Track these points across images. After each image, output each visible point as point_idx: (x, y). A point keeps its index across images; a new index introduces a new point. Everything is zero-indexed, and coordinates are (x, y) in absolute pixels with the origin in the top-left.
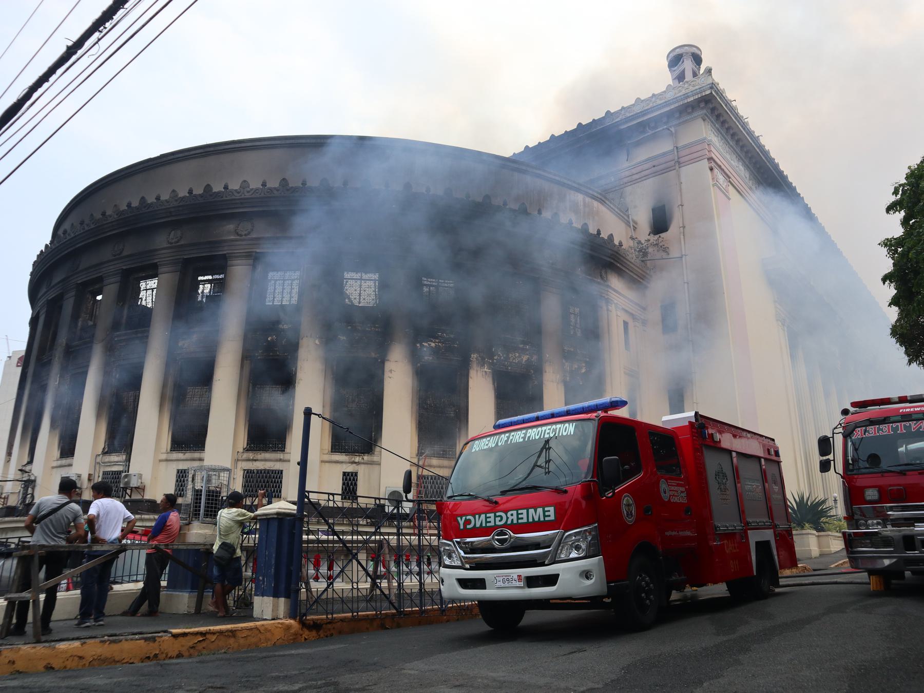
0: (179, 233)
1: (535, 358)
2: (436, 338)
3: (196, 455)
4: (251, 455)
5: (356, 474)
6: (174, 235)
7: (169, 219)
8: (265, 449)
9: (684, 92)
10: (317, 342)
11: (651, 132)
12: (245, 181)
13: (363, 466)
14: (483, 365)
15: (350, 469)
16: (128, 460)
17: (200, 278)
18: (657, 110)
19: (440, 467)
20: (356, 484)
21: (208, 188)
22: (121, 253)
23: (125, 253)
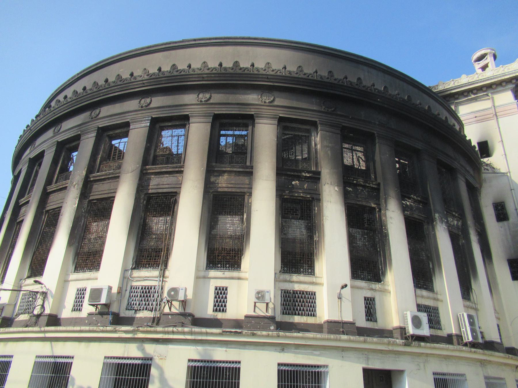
0: (208, 96)
1: (460, 223)
2: (410, 198)
3: (235, 274)
4: (287, 276)
5: (374, 299)
6: (204, 96)
7: (201, 83)
8: (297, 272)
9: (500, 72)
10: (336, 189)
11: (473, 96)
12: (268, 63)
13: (378, 293)
14: (442, 223)
15: (369, 294)
17: (222, 132)
18: (481, 82)
19: (428, 298)
21: (236, 63)
22: (149, 105)
23: (152, 106)
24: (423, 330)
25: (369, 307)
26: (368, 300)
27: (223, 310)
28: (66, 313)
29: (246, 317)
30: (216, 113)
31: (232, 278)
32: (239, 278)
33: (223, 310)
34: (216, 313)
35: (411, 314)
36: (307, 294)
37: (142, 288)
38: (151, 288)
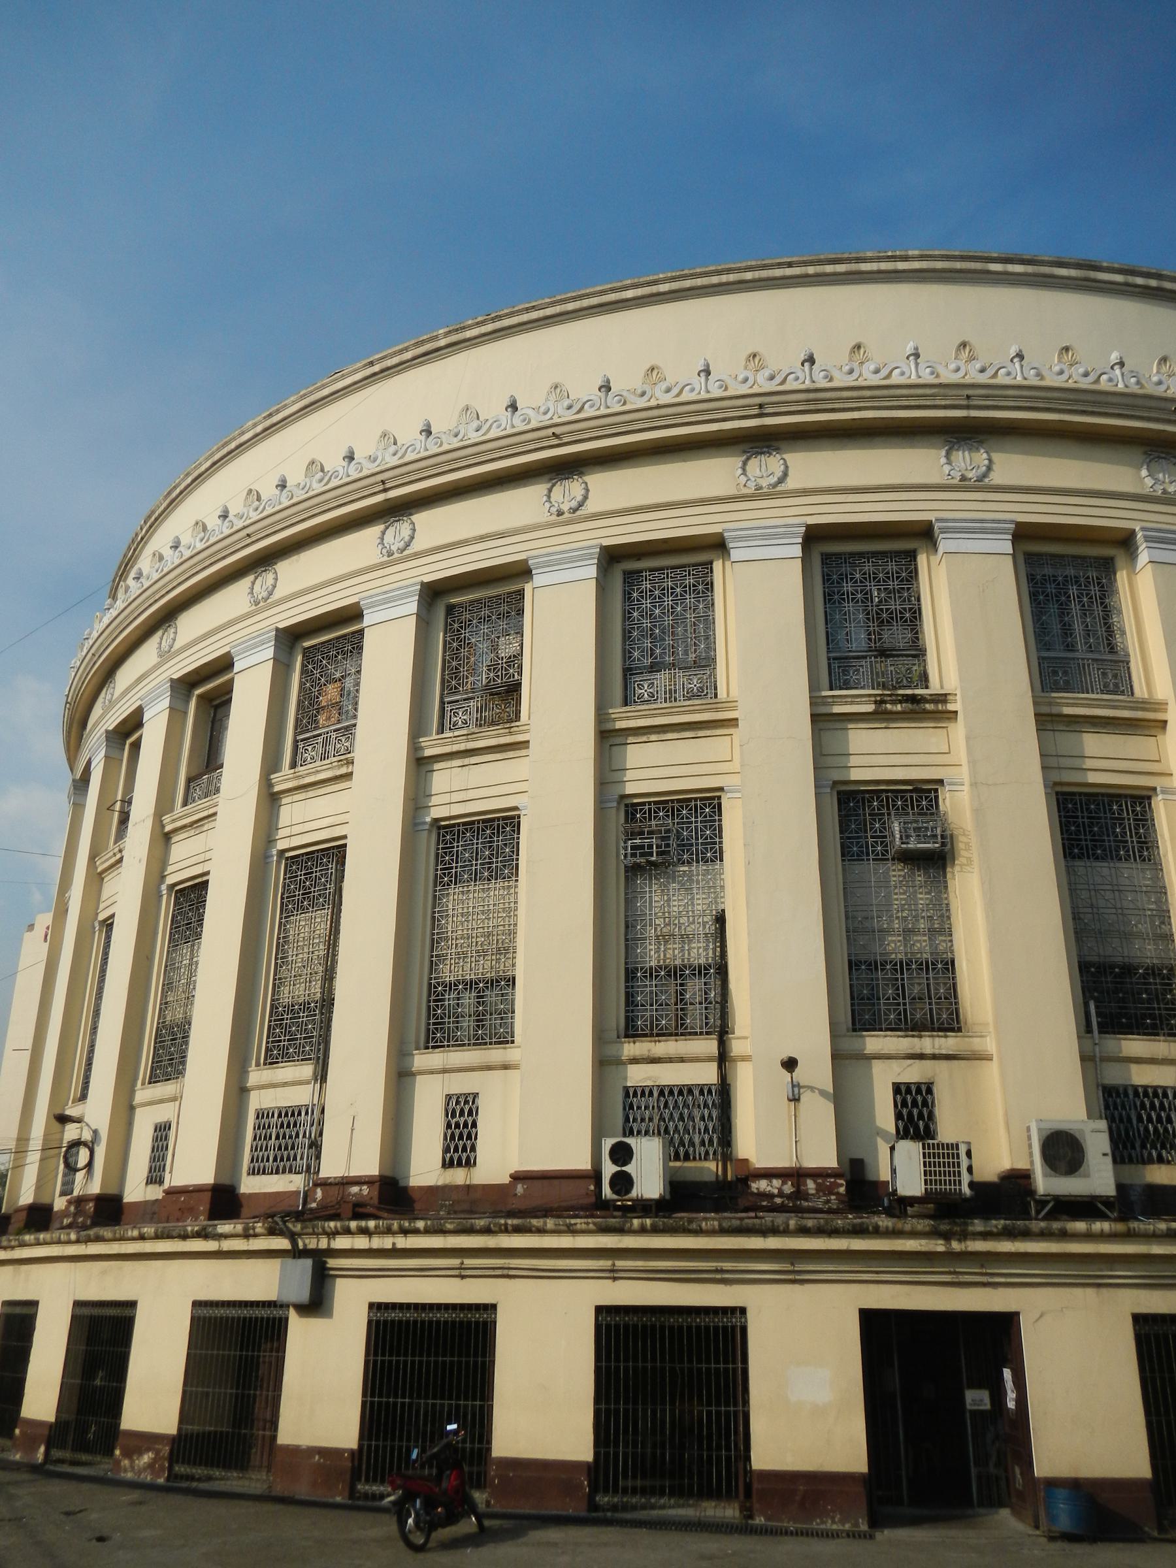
3: (495, 1054)
5: (929, 1091)
15: (912, 1073)
16: (321, 1076)
20: (931, 1116)
24: (1087, 1175)
25: (910, 1114)
26: (908, 1091)
27: (468, 1158)
28: (136, 1191)
29: (517, 1177)
30: (427, 579)
31: (489, 1068)
32: (506, 1067)
33: (468, 1158)
34: (450, 1171)
35: (1039, 1130)
36: (702, 1093)
37: (280, 1116)
38: (300, 1114)
